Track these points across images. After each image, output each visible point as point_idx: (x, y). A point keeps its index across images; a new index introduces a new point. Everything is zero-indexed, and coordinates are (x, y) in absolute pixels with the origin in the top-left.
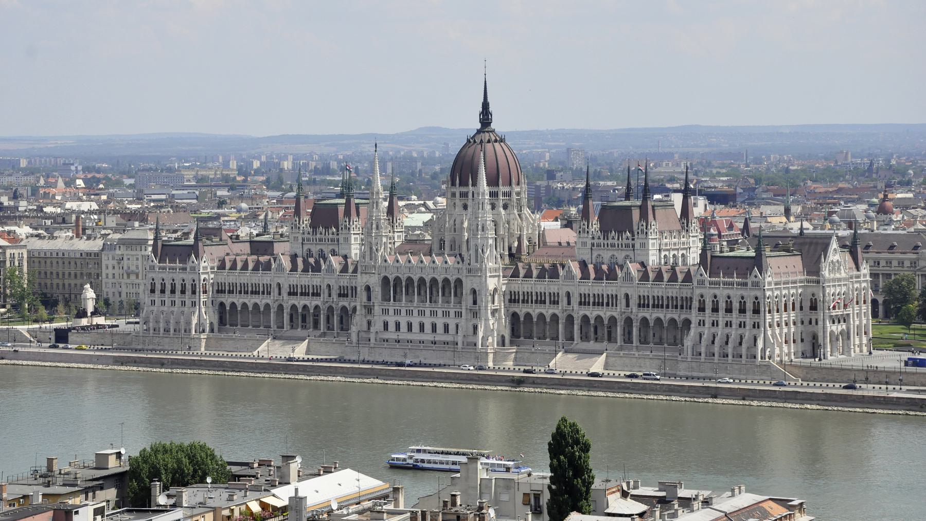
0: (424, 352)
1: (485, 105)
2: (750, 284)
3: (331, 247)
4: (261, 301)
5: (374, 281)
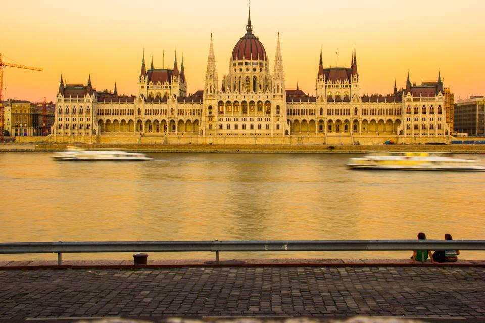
0: (250, 139)
1: (249, 22)
2: (437, 99)
3: (165, 91)
4: (127, 118)
5: (214, 104)
